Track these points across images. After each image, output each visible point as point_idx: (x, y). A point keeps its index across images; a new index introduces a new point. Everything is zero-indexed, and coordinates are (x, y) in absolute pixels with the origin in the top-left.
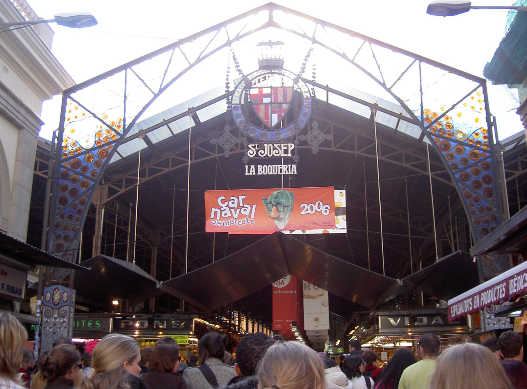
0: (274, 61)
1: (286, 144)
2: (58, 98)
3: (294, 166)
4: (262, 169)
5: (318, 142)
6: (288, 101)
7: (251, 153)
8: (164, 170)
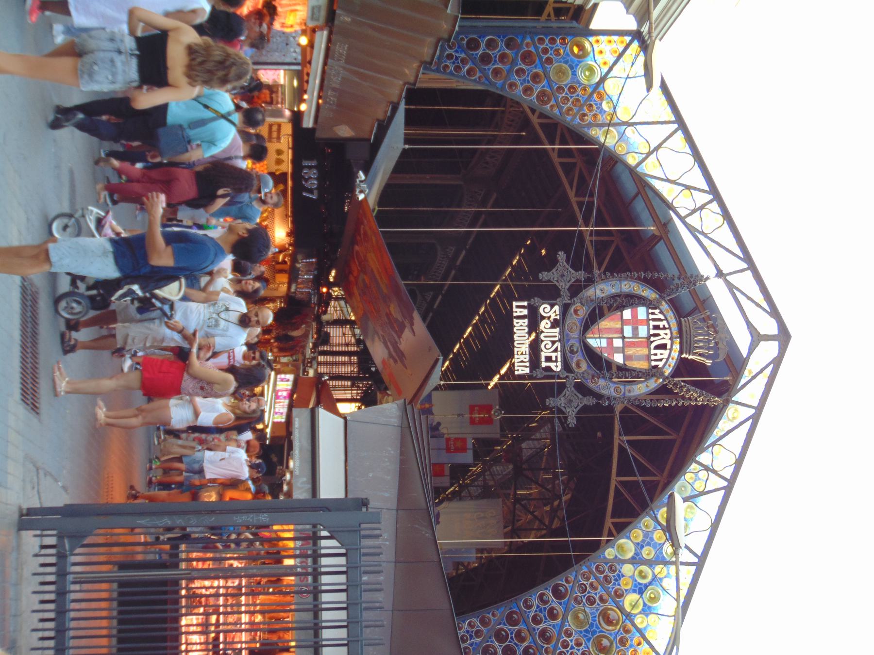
0: (688, 340)
1: (559, 359)
2: (631, 24)
3: (527, 371)
4: (521, 326)
5: (563, 405)
6: (628, 363)
7: (545, 309)
8: (572, 188)
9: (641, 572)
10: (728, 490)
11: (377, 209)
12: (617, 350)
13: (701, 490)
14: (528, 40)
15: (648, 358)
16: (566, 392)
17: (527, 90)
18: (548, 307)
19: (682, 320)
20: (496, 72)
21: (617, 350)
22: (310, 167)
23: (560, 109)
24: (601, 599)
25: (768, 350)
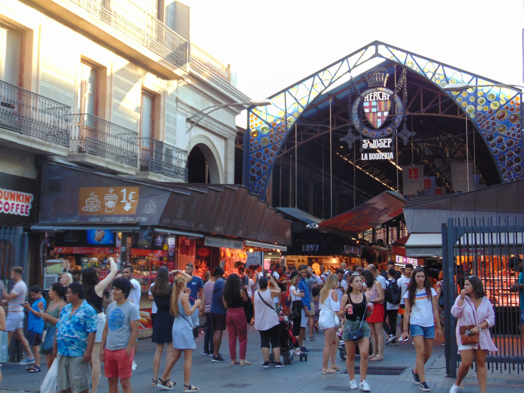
1: (386, 139)
2: (244, 112)
3: (392, 153)
7: (365, 146)
9: (481, 102)
10: (443, 65)
11: (323, 219)
12: (382, 114)
13: (444, 77)
14: (251, 155)
15: (385, 101)
16: (401, 136)
17: (272, 155)
18: (364, 145)
19: (369, 87)
20: (264, 168)
21: (382, 114)
22: (305, 248)
23: (279, 141)
24: (493, 119)
25: (382, 50)
